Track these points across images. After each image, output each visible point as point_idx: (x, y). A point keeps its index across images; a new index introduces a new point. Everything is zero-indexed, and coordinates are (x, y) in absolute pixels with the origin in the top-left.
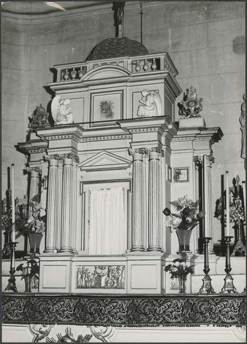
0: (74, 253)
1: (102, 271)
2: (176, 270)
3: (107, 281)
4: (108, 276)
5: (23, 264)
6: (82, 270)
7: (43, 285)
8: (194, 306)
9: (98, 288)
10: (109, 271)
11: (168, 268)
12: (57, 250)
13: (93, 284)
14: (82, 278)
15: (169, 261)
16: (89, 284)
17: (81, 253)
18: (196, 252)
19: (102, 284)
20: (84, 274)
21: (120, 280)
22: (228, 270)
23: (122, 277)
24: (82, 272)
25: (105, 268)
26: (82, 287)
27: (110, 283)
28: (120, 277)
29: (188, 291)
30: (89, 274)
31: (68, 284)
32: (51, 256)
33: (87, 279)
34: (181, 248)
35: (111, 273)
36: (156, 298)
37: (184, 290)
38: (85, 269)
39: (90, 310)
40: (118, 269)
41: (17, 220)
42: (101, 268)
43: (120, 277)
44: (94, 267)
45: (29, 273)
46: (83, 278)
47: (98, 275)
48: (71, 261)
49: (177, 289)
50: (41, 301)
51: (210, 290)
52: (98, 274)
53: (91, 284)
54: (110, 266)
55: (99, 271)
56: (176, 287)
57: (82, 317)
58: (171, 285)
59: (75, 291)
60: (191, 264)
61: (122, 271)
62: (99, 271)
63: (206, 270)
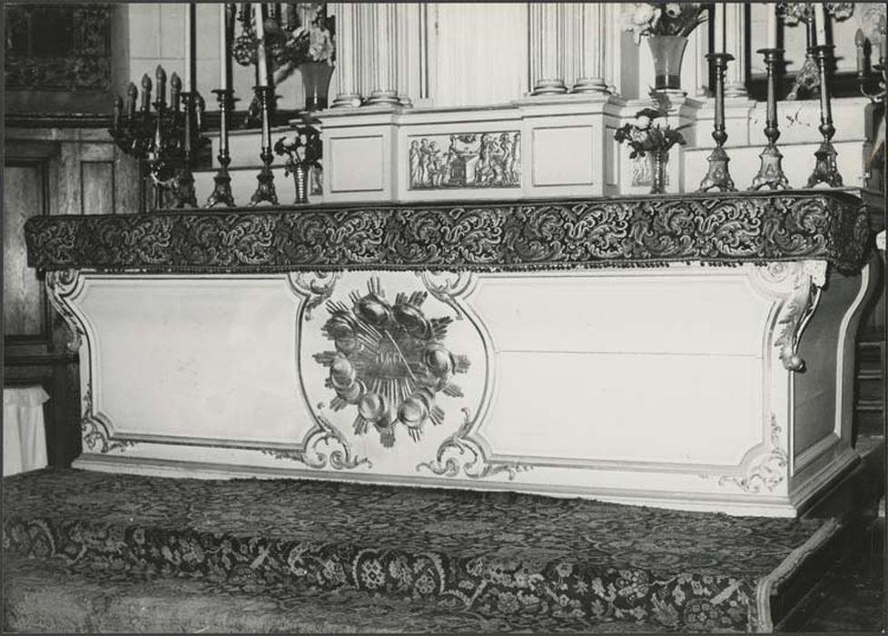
0: (402, 105)
1: (468, 145)
2: (643, 137)
3: (480, 171)
4: (482, 158)
5: (284, 138)
6: (420, 145)
7: (331, 186)
8: (789, 216)
9: (459, 187)
10: (483, 147)
11: (622, 135)
12: (362, 99)
13: (448, 177)
14: (421, 163)
15: (627, 114)
16: (437, 180)
17: (418, 105)
18: (702, 92)
19: (468, 176)
20: (427, 156)
21: (508, 166)
22: (773, 133)
23: (514, 159)
24: (421, 150)
25: (474, 139)
26: (422, 187)
27: (487, 175)
28: (510, 160)
29: (672, 189)
30: (438, 155)
31: (388, 176)
32: (347, 115)
33: (432, 166)
34: (660, 81)
35: (487, 149)
36: (592, 203)
37: (662, 185)
38: (427, 144)
39: (802, 224)
40: (503, 139)
41: (268, 30)
42: (466, 138)
43: (510, 160)
44: (448, 137)
45: (303, 157)
46: (425, 165)
47: (459, 157)
48: (394, 124)
49: (646, 184)
50: (675, 206)
51: (725, 183)
52: (458, 153)
53: (443, 178)
54: (485, 134)
55: (460, 146)
56: (644, 179)
57: (779, 243)
58: (632, 175)
59: (406, 196)
60: (680, 121)
61: (514, 145)
62: (460, 146)
63: (721, 137)
